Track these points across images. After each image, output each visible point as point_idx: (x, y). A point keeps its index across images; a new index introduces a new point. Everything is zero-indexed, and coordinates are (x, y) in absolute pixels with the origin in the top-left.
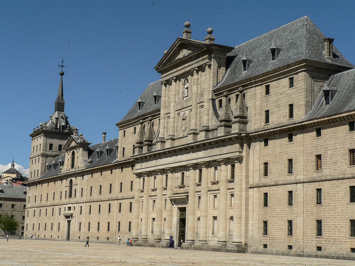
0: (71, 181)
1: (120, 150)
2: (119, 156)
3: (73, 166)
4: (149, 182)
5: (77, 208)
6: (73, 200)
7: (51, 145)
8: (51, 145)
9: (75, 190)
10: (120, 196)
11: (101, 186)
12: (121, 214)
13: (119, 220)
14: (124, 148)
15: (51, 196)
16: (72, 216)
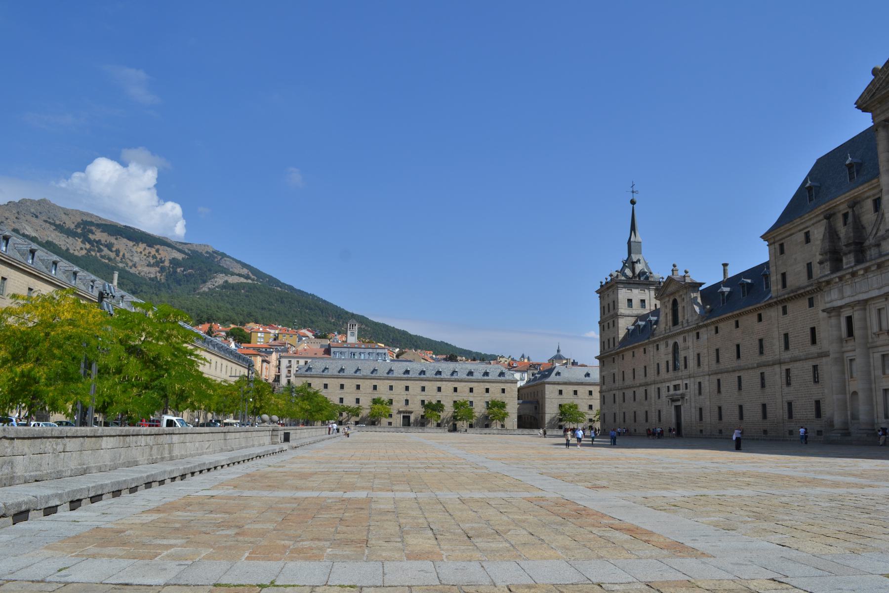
0: (676, 345)
1: (775, 278)
2: (773, 288)
3: (675, 322)
4: (865, 319)
5: (692, 385)
6: (682, 373)
7: (630, 301)
8: (630, 301)
9: (685, 358)
10: (787, 355)
11: (738, 346)
12: (791, 388)
13: (790, 398)
14: (784, 275)
15: (640, 372)
16: (683, 396)
